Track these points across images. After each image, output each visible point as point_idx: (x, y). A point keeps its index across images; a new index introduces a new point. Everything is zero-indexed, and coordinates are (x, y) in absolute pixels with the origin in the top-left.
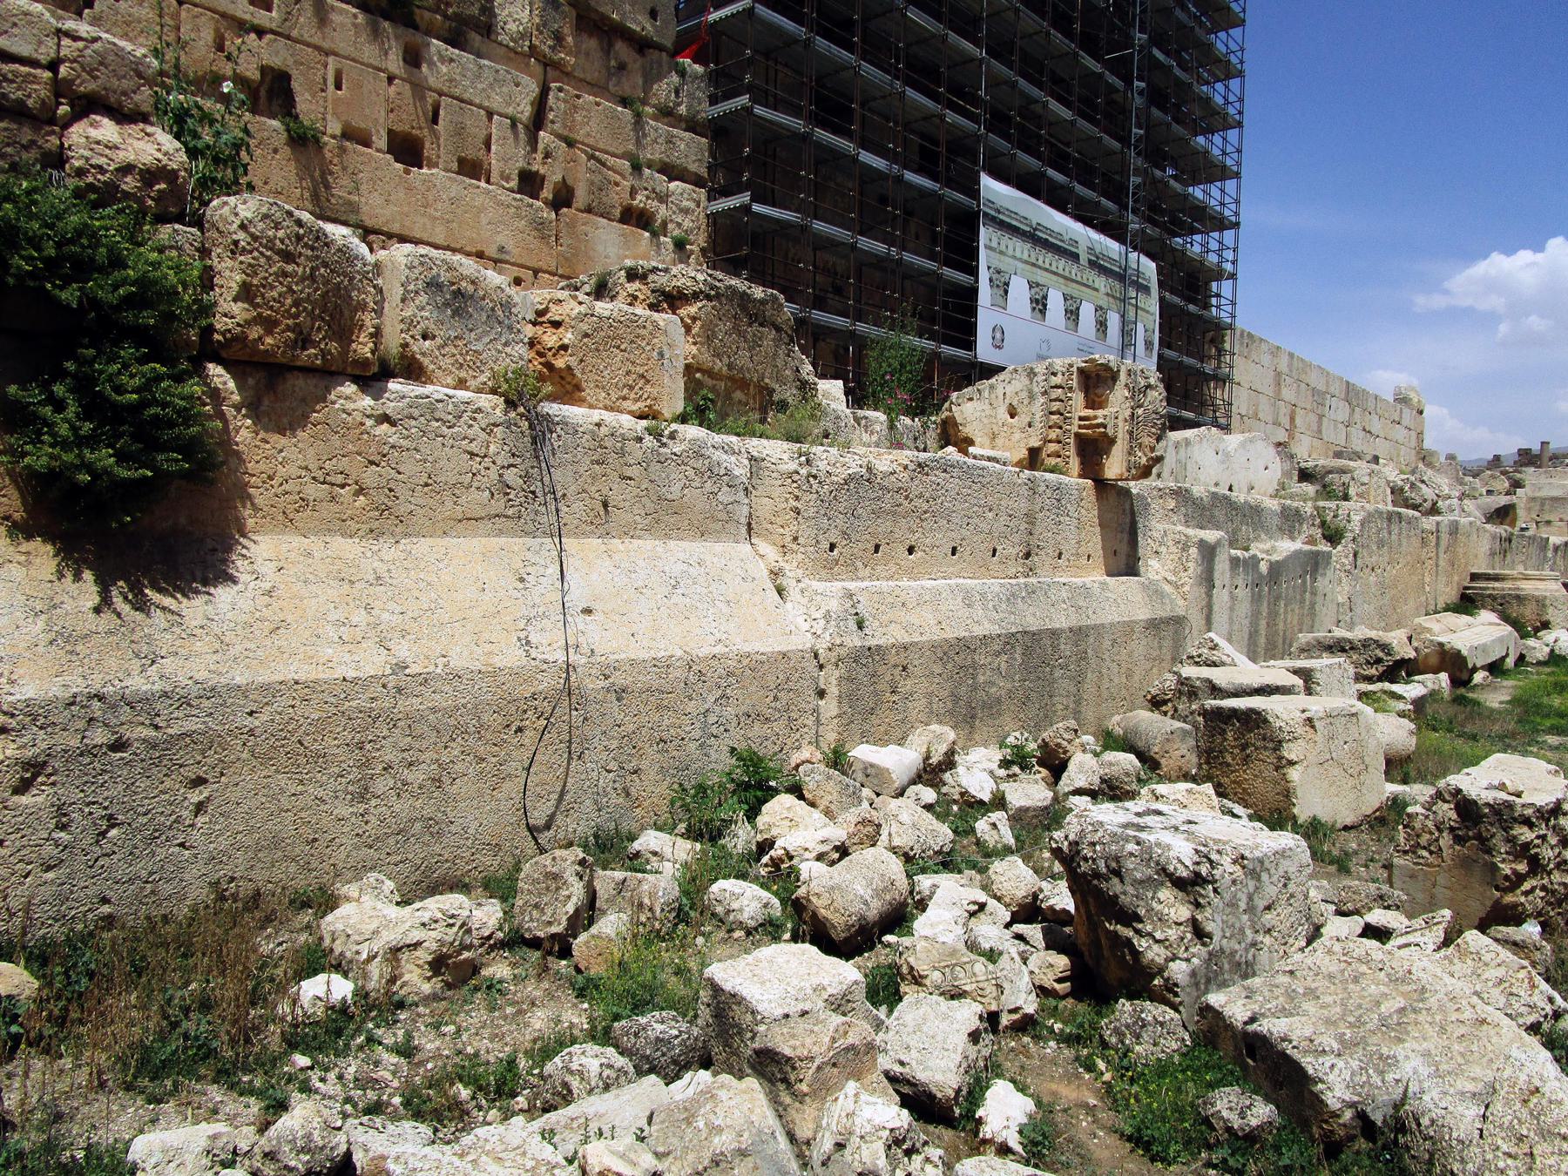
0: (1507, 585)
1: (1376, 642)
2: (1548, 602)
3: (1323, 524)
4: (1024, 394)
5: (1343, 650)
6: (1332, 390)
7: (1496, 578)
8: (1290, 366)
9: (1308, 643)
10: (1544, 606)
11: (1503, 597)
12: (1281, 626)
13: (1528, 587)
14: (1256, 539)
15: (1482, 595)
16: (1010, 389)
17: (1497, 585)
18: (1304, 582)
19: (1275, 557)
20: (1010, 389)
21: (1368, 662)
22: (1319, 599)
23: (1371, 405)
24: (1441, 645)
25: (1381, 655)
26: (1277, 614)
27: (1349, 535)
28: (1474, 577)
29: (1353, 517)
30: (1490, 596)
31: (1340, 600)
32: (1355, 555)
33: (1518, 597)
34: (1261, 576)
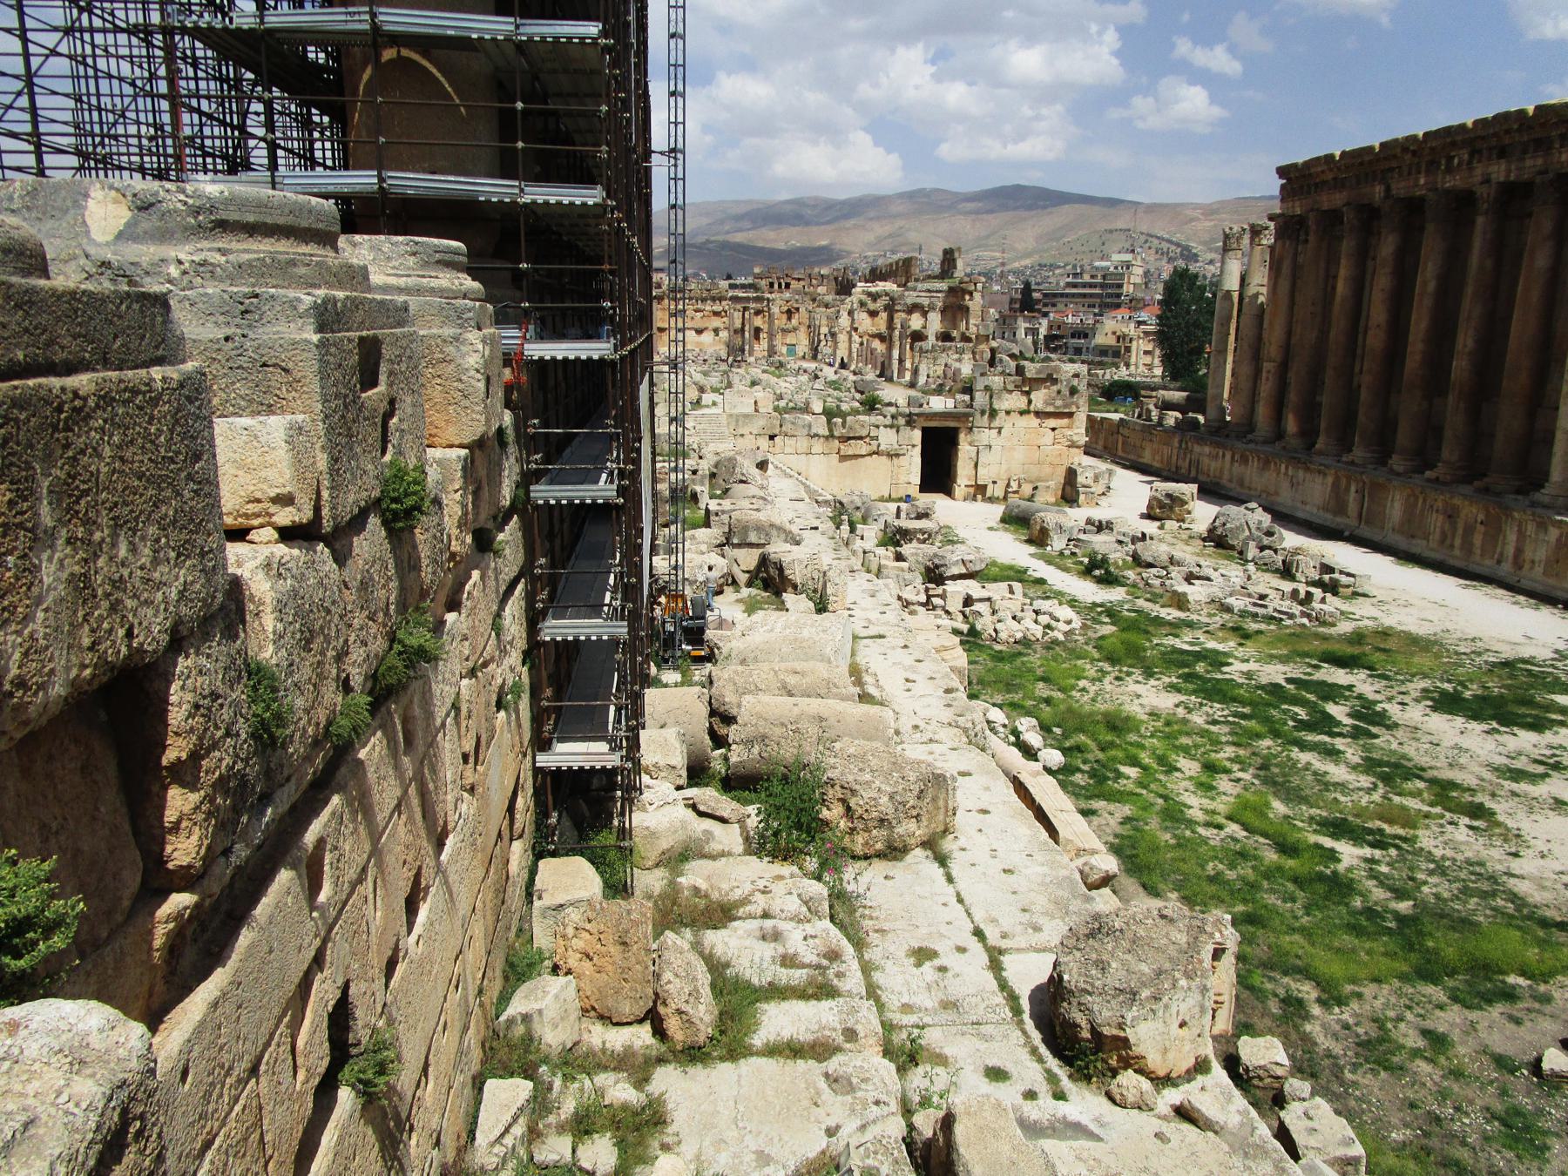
4: (1197, 1009)
16: (1183, 1007)
20: (1183, 1007)
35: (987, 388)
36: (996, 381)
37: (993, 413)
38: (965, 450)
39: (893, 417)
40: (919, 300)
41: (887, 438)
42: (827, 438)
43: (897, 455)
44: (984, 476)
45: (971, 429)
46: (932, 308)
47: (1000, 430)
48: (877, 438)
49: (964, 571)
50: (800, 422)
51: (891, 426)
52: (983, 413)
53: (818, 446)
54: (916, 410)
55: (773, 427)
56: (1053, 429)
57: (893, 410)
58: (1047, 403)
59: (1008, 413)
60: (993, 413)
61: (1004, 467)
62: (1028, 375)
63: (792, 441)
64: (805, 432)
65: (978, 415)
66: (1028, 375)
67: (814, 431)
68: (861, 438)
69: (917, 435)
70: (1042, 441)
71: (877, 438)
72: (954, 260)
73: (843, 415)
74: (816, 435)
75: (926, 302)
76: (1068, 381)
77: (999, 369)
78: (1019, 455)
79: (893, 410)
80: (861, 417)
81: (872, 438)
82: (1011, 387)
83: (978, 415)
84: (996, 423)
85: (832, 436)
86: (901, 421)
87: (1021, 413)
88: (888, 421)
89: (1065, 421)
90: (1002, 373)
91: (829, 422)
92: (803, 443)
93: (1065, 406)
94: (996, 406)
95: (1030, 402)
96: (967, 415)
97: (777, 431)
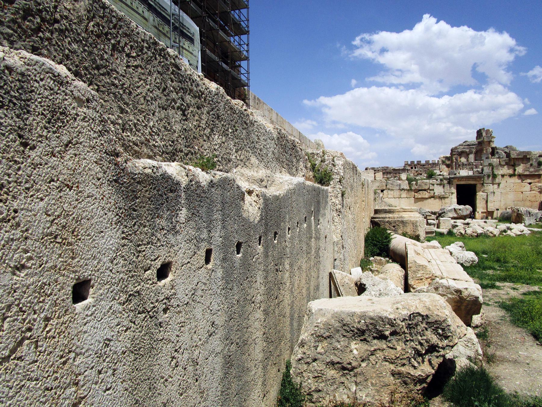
0: (396, 215)
1: (425, 317)
2: (418, 224)
3: (313, 167)
5: (382, 337)
6: (294, 134)
7: (390, 212)
8: (277, 119)
9: (328, 326)
10: (416, 226)
11: (395, 222)
12: (287, 300)
13: (406, 216)
14: (245, 162)
15: (384, 222)
17: (390, 215)
18: (309, 226)
19: (272, 191)
21: (418, 354)
22: (322, 244)
23: (308, 143)
24: (459, 291)
25: (435, 339)
26: (280, 284)
27: (336, 177)
28: (376, 212)
29: (337, 162)
30: (388, 222)
31: (336, 240)
32: (343, 195)
33: (402, 222)
34: (246, 224)
35: (490, 165)
36: (495, 161)
37: (494, 176)
38: (480, 196)
39: (441, 180)
40: (464, 150)
41: (438, 190)
42: (408, 190)
43: (444, 198)
44: (491, 207)
45: (483, 184)
46: (471, 152)
47: (499, 184)
48: (433, 190)
49: (456, 216)
50: (395, 184)
51: (440, 185)
52: (488, 176)
53: (404, 194)
54: (453, 176)
55: (383, 186)
56: (530, 183)
57: (441, 177)
58: (525, 170)
59: (503, 176)
60: (494, 176)
61: (503, 203)
62: (512, 156)
63: (392, 192)
64: (398, 188)
65: (486, 178)
66: (512, 156)
67: (402, 187)
68: (425, 190)
69: (454, 191)
70: (523, 189)
71: (433, 190)
72: (482, 134)
73: (416, 180)
74: (403, 189)
75: (468, 150)
76: (536, 159)
77: (497, 156)
78: (511, 197)
79: (441, 177)
80: (425, 181)
81: (431, 190)
82: (503, 163)
83: (486, 178)
84: (497, 181)
85: (411, 190)
86: (445, 182)
87: (511, 176)
88: (439, 182)
89: (537, 180)
90: (499, 158)
91: (409, 184)
92: (397, 193)
93: (535, 171)
94: (496, 173)
95: (515, 170)
96: (480, 178)
97: (384, 188)
